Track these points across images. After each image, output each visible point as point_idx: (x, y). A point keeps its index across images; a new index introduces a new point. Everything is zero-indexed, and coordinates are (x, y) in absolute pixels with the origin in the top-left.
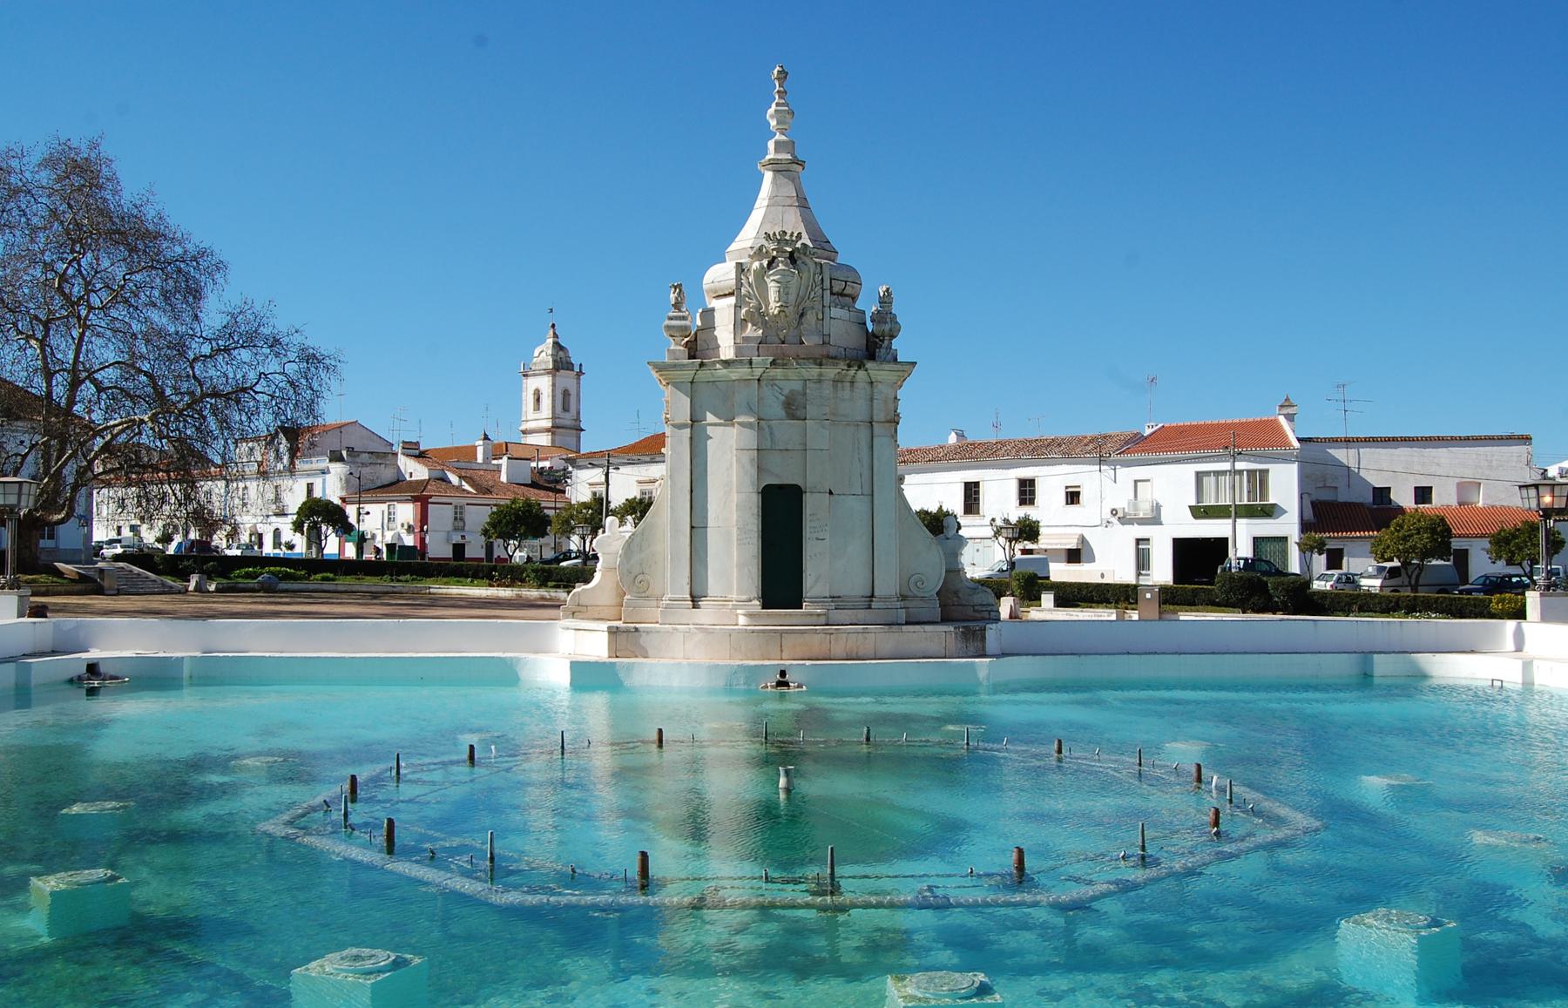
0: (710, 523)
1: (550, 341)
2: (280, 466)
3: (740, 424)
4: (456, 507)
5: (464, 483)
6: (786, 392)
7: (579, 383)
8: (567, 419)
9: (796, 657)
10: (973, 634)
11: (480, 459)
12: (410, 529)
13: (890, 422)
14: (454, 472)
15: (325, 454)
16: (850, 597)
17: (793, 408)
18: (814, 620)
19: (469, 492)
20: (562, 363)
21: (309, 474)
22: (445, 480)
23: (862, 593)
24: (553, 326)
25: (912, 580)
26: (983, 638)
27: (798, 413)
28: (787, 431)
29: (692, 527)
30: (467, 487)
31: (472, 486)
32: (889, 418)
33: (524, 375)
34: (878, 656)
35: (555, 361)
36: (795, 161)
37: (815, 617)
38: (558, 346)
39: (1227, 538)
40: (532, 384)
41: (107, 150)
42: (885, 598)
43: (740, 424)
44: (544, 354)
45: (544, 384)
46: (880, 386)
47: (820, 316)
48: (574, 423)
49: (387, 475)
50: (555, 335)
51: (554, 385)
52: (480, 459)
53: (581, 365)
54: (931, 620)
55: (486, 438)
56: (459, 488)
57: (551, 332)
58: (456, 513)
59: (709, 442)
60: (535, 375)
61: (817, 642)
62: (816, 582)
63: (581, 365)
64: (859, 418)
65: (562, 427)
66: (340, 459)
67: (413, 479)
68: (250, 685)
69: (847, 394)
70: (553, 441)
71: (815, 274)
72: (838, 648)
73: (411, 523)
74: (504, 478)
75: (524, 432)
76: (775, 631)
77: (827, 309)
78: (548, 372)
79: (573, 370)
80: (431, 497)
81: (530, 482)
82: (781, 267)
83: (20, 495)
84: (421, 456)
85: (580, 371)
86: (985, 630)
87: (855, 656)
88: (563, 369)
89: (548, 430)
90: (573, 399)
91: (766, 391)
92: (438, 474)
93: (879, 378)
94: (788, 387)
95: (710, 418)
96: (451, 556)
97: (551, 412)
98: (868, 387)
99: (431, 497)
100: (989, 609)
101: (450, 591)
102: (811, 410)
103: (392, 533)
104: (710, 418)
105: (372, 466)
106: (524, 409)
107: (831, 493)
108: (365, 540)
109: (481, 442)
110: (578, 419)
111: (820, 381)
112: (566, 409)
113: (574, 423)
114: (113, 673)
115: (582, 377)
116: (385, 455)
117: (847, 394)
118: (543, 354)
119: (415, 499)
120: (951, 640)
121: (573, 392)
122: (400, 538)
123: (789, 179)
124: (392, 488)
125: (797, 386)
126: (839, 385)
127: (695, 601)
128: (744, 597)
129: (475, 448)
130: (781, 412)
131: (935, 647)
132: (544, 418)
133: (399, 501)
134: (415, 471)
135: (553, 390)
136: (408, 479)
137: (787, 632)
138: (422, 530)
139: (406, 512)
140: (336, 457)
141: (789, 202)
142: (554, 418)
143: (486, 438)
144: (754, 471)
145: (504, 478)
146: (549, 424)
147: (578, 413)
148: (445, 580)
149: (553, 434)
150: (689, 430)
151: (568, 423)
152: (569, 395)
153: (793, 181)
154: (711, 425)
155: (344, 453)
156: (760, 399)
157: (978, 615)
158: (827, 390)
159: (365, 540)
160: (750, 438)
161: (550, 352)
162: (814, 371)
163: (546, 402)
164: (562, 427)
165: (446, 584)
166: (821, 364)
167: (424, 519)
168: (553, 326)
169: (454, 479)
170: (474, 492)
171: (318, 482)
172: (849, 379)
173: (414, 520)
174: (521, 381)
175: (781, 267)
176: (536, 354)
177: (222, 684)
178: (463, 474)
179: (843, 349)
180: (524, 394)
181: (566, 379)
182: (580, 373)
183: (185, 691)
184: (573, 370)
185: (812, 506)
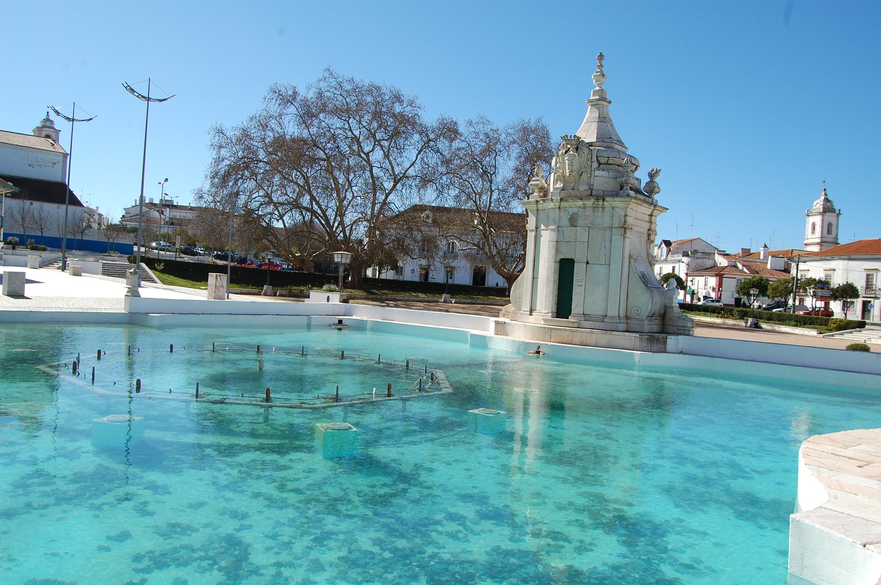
0: (540, 276)
1: (823, 198)
2: (662, 259)
3: (551, 229)
4: (738, 280)
5: (744, 268)
6: (570, 213)
7: (838, 219)
8: (830, 238)
9: (564, 342)
10: (657, 340)
11: (762, 257)
12: (714, 289)
13: (621, 228)
14: (740, 263)
15: (680, 253)
16: (595, 315)
17: (573, 221)
18: (570, 325)
19: (745, 273)
20: (828, 208)
21: (674, 262)
22: (736, 266)
23: (602, 314)
24: (825, 190)
25: (634, 309)
26: (665, 343)
27: (575, 224)
28: (569, 232)
29: (534, 278)
30: (746, 270)
31: (748, 270)
32: (620, 226)
33: (808, 216)
34: (598, 345)
35: (823, 208)
36: (604, 99)
37: (571, 324)
38: (826, 200)
39: (863, 301)
40: (811, 220)
41: (545, 122)
42: (612, 317)
43: (551, 229)
44: (818, 205)
45: (817, 220)
46: (617, 209)
47: (589, 175)
48: (834, 240)
49: (709, 263)
50: (826, 194)
51: (823, 220)
52: (762, 257)
53: (840, 210)
54: (640, 331)
55: (765, 246)
56: (742, 271)
57: (823, 193)
58: (738, 283)
59: (542, 238)
60: (813, 215)
61: (566, 336)
62: (576, 307)
63: (840, 210)
64: (606, 226)
65: (827, 242)
66: (687, 255)
67: (721, 265)
68: (383, 332)
69: (600, 213)
70: (821, 249)
71: (587, 155)
72: (576, 340)
73: (714, 287)
74: (769, 267)
75: (806, 245)
76: (549, 328)
77: (593, 172)
78: (820, 214)
79: (835, 212)
80: (724, 274)
81: (783, 269)
82: (571, 153)
83: (342, 258)
84: (726, 255)
85: (839, 213)
86: (666, 338)
87: (584, 344)
88: (829, 212)
89: (818, 244)
90: (834, 228)
91: (563, 213)
92: (733, 264)
93: (616, 205)
94: (571, 211)
95: (543, 227)
96: (734, 303)
97: (820, 234)
98: (612, 210)
99: (724, 274)
100: (685, 329)
101: (695, 318)
102: (580, 222)
103: (706, 291)
104: (543, 227)
105: (702, 259)
106: (806, 233)
107: (588, 263)
108: (695, 294)
109: (762, 249)
110: (836, 238)
111: (585, 208)
112: (829, 232)
113: (834, 240)
114: (347, 324)
115: (840, 216)
116: (709, 255)
117: (600, 213)
118: (818, 204)
119: (716, 275)
120: (637, 341)
121: (834, 224)
122: (709, 294)
123: (597, 108)
124: (709, 270)
125: (575, 210)
126: (596, 209)
127: (531, 311)
128: (546, 311)
129: (759, 253)
130: (568, 223)
131: (629, 344)
132: (816, 237)
133: (710, 276)
134: (722, 262)
135: (822, 223)
136: (719, 265)
137: (556, 329)
138: (719, 290)
139: (713, 281)
140: (685, 254)
141: (594, 120)
142: (822, 237)
143: (765, 246)
144: (554, 252)
145: (769, 267)
146: (819, 240)
147: (837, 235)
148: (699, 313)
149: (821, 245)
150: (534, 233)
151: (830, 240)
152: (832, 225)
153: (599, 109)
154: (542, 230)
155: (689, 253)
156: (560, 217)
157: (679, 332)
158: (589, 212)
159: (695, 294)
160: (554, 234)
161: (822, 203)
162: (580, 203)
163: (818, 229)
164: (827, 242)
165: (699, 315)
166: (582, 199)
167: (720, 284)
168: (825, 190)
169: (740, 266)
170: (749, 273)
171: (677, 266)
172: (601, 206)
173: (716, 285)
174: (806, 219)
175: (571, 153)
176: (815, 204)
177: (380, 332)
178: (745, 264)
179: (602, 192)
180: (807, 225)
181: (830, 217)
182: (839, 214)
183: (368, 333)
184: (835, 212)
185: (578, 268)
